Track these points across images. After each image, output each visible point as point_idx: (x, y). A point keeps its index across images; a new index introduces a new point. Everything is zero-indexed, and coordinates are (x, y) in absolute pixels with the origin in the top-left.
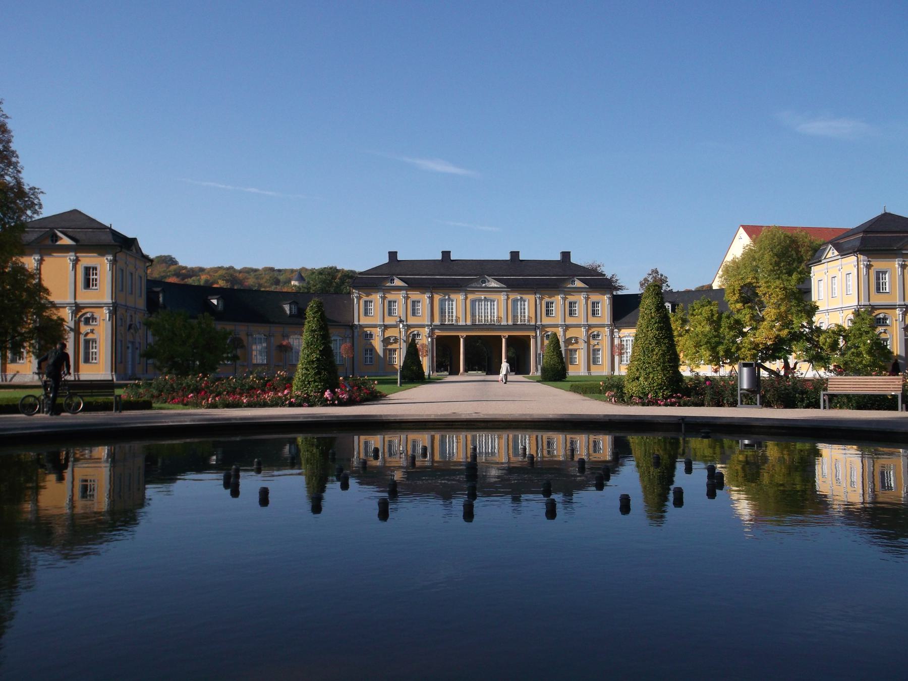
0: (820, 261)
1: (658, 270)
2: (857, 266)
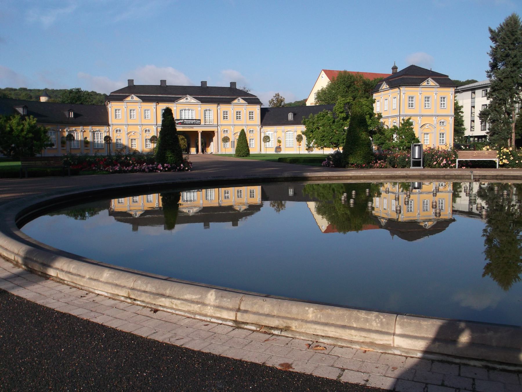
1: (279, 94)
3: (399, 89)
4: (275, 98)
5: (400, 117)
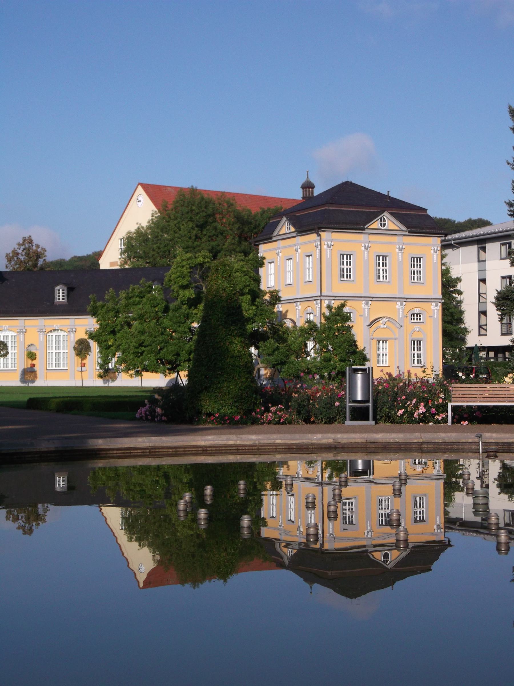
0: (271, 238)
1: (33, 238)
2: (319, 246)
3: (319, 235)
4: (22, 248)
5: (321, 300)
